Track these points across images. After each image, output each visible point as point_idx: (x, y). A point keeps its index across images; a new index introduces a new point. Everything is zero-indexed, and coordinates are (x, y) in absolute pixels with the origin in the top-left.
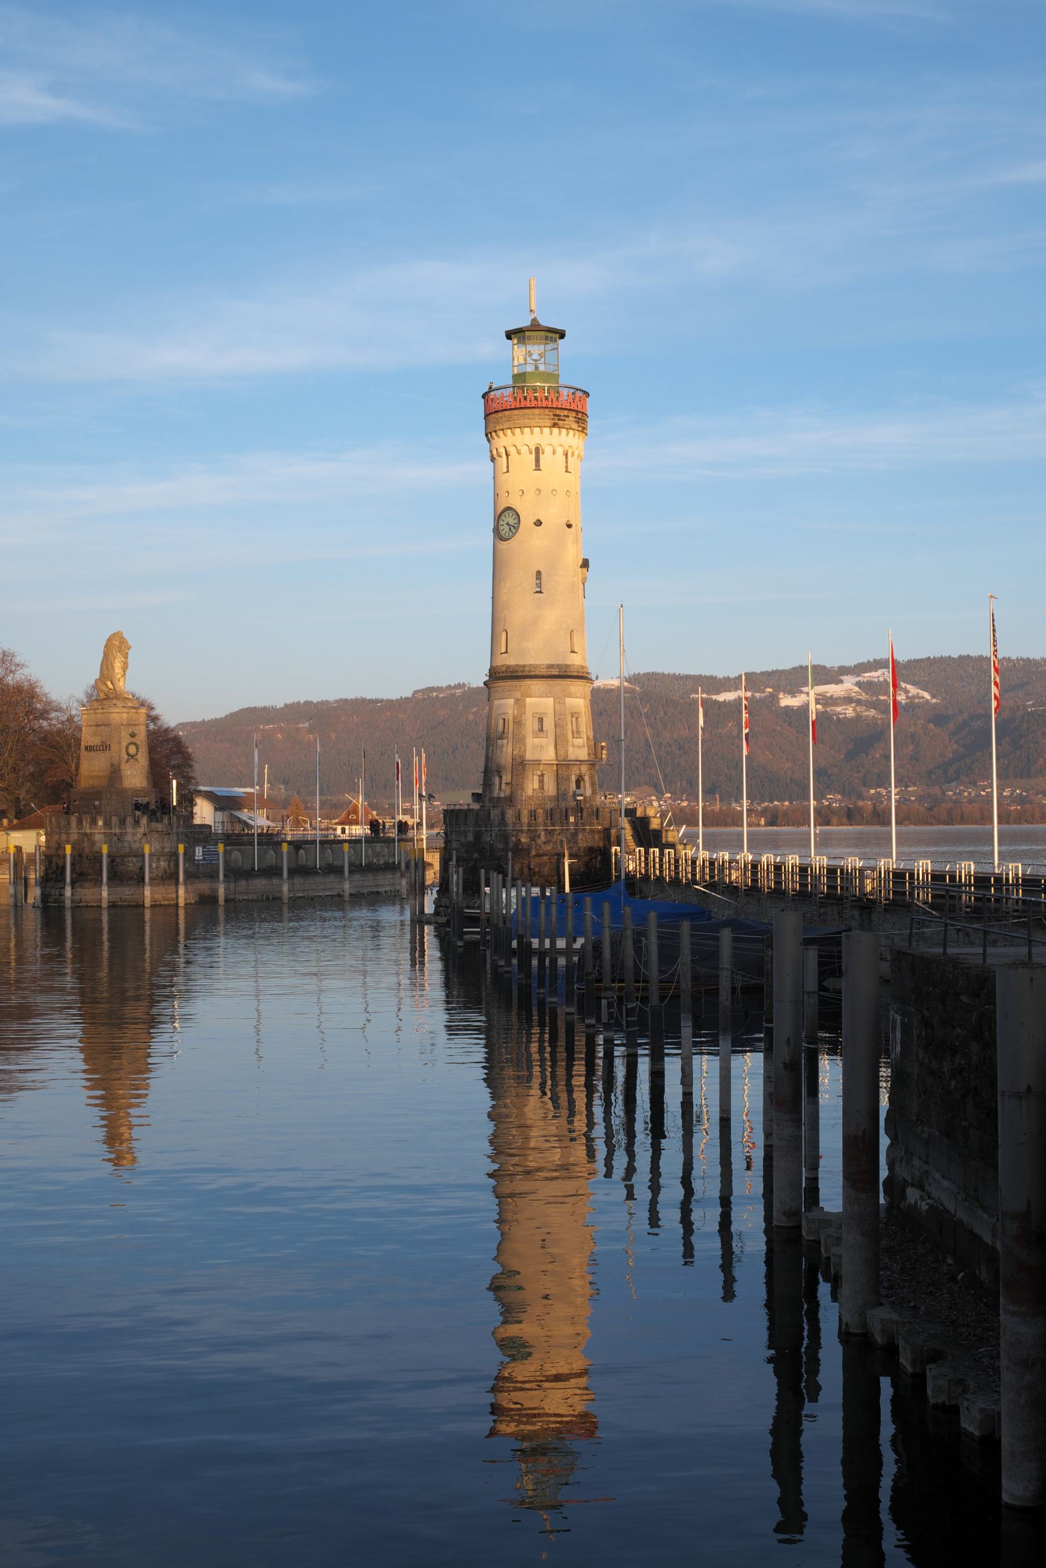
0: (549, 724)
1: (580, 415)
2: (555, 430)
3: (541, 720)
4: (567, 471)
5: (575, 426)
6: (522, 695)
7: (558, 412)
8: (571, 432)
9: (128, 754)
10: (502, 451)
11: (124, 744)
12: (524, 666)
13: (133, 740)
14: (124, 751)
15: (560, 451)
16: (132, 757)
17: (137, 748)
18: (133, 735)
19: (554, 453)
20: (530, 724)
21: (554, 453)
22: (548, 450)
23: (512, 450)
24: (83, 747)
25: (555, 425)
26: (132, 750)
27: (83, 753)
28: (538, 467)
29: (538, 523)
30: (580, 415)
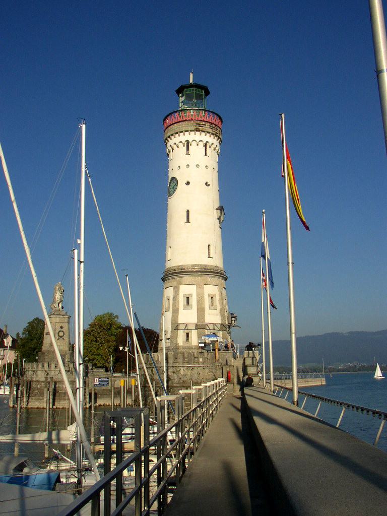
0: (194, 301)
1: (213, 126)
2: (198, 133)
3: (188, 298)
4: (206, 155)
5: (210, 130)
6: (178, 284)
7: (199, 122)
8: (208, 134)
9: (59, 336)
10: (170, 148)
11: (57, 331)
12: (179, 266)
13: (62, 330)
14: (57, 335)
15: (201, 144)
16: (61, 337)
17: (64, 333)
18: (61, 327)
19: (198, 145)
20: (182, 301)
21: (198, 145)
22: (194, 144)
23: (175, 147)
24: (45, 333)
25: (197, 130)
26: (61, 334)
27: (45, 335)
28: (188, 153)
29: (188, 183)
30: (213, 126)
